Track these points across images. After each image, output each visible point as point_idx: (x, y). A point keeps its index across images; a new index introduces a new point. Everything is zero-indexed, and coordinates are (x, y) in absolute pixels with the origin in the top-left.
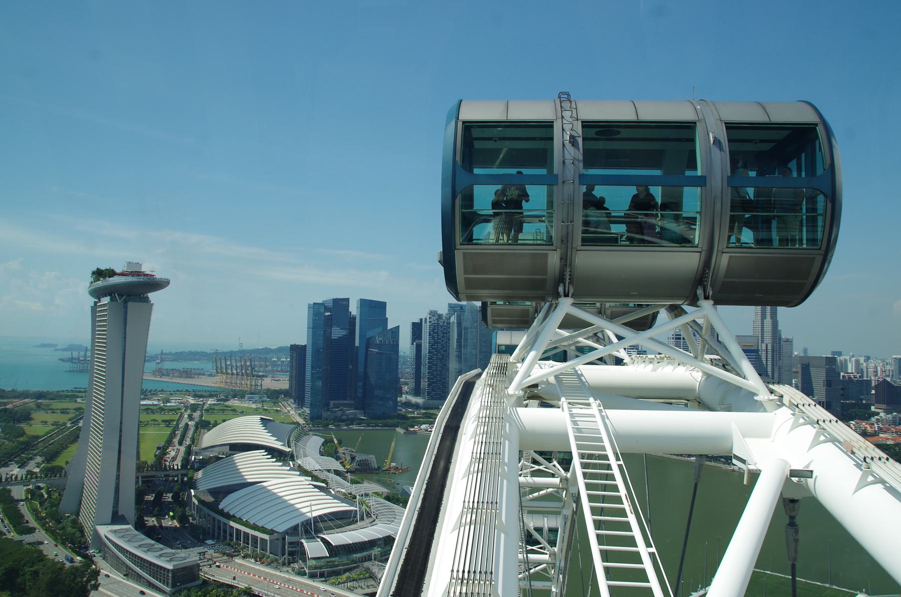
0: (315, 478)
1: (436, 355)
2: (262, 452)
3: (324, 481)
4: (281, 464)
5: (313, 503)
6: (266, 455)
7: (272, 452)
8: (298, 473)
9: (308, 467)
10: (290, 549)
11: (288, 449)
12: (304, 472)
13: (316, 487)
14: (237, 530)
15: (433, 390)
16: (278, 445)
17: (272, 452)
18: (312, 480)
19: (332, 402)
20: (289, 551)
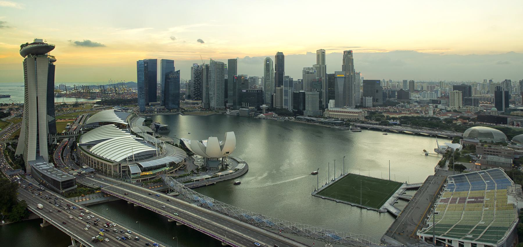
0: (138, 136)
1: (197, 82)
2: (114, 125)
3: (141, 137)
4: (121, 130)
5: (134, 148)
6: (115, 126)
7: (119, 125)
8: (130, 134)
9: (135, 132)
10: (123, 170)
11: (126, 124)
12: (133, 133)
13: (136, 140)
14: (98, 161)
15: (196, 96)
16: (122, 122)
17: (119, 125)
18: (136, 137)
19: (150, 104)
20: (122, 170)
